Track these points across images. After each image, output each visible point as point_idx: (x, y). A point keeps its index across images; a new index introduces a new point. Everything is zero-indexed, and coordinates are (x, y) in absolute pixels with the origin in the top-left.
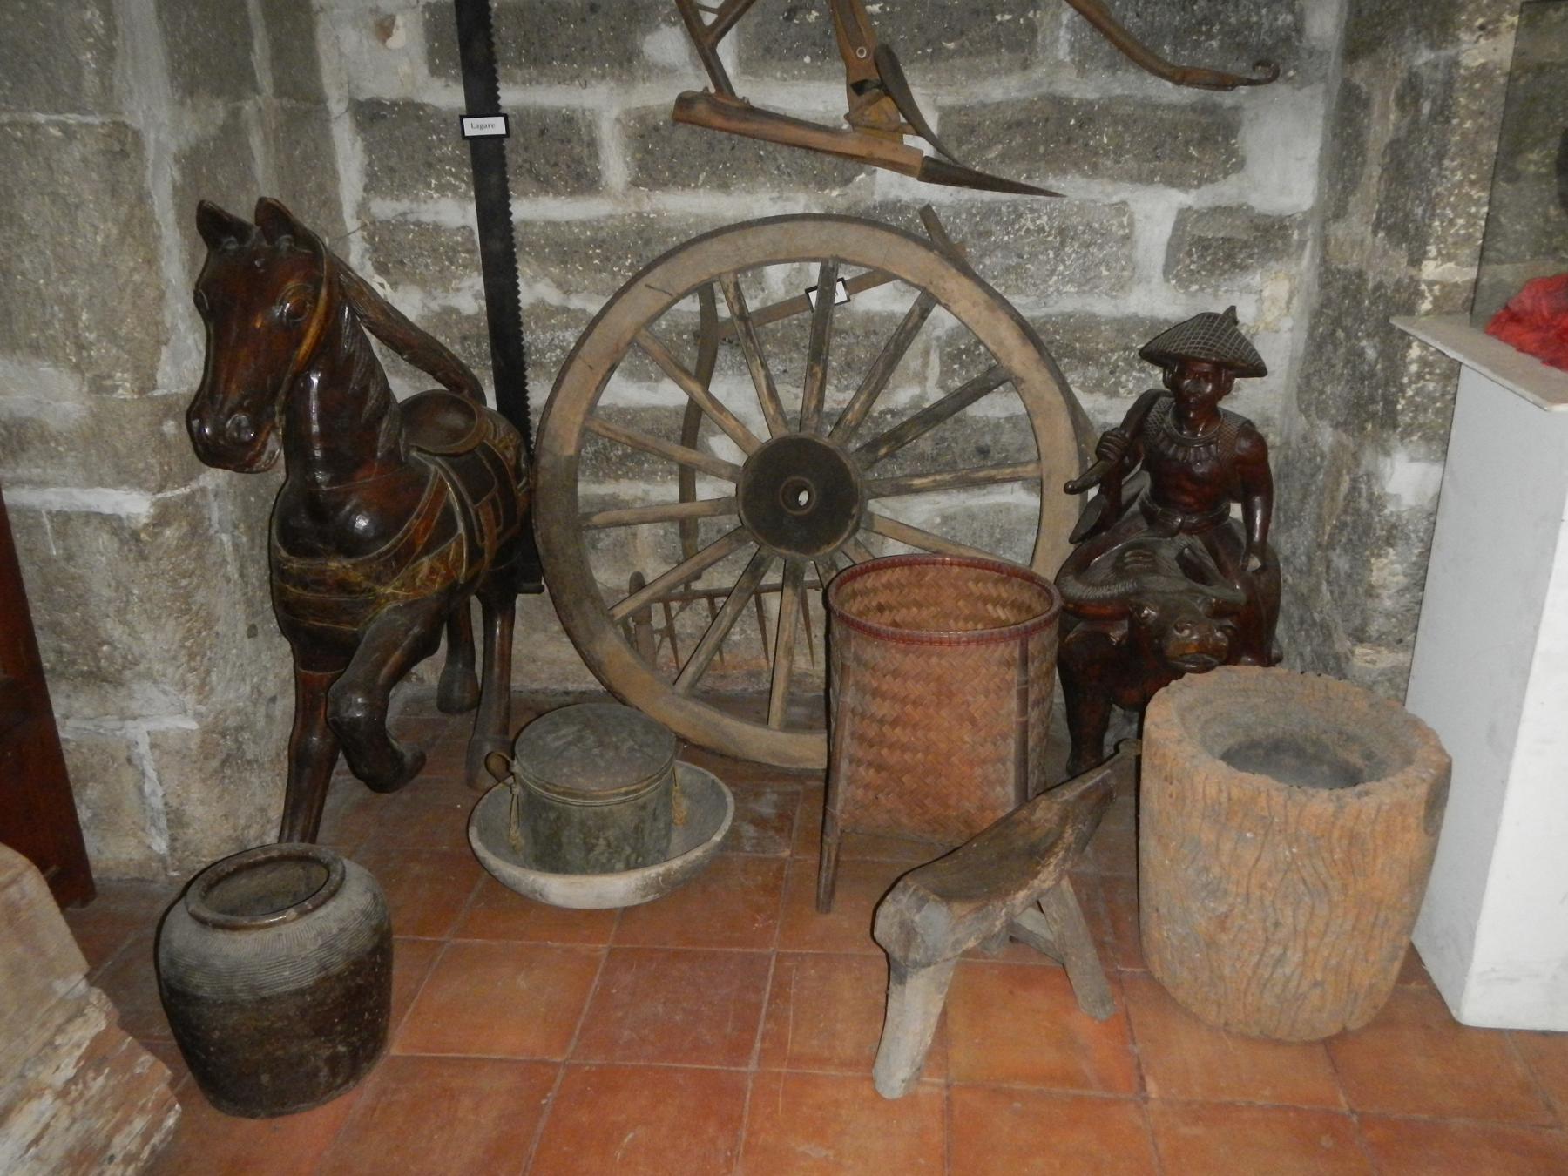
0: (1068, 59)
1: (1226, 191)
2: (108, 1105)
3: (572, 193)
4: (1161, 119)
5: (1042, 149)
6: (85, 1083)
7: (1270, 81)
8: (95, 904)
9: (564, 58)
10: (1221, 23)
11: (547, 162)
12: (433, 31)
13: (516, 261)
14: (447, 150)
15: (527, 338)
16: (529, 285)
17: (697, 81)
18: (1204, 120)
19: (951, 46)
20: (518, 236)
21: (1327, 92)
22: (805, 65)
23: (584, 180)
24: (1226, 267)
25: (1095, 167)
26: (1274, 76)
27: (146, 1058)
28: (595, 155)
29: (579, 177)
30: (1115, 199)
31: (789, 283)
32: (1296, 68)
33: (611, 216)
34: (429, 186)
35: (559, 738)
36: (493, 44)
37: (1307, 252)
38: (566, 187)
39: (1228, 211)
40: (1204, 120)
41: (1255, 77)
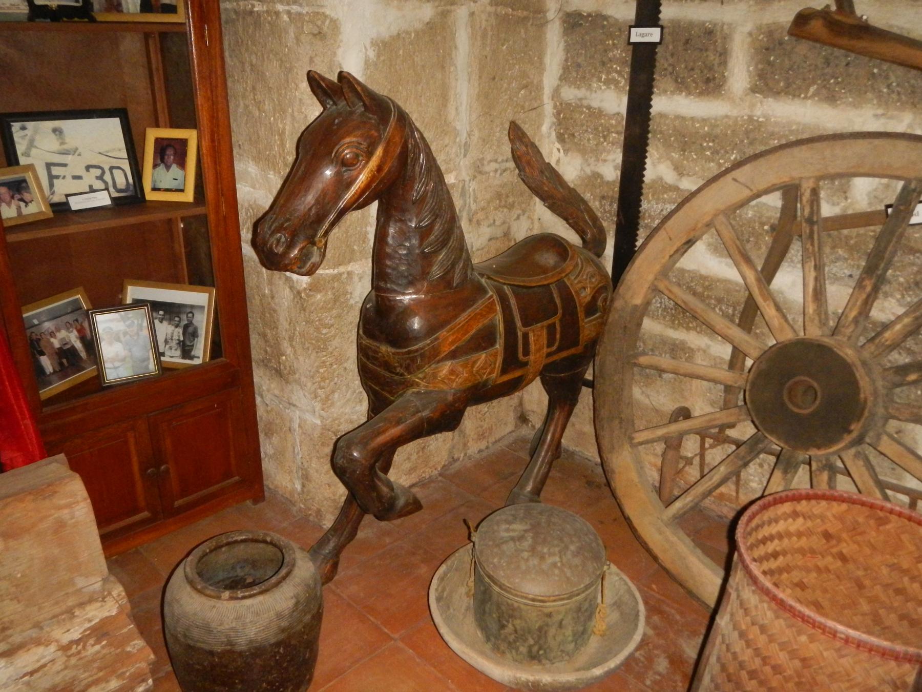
2: (96, 665)
3: (701, 94)
6: (84, 647)
8: (261, 505)
11: (686, 67)
13: (647, 145)
14: (617, 53)
15: (645, 205)
16: (654, 165)
20: (652, 125)
23: (711, 83)
27: (139, 643)
28: (724, 63)
29: (708, 81)
31: (874, 196)
33: (727, 116)
34: (600, 80)
35: (508, 530)
38: (696, 88)
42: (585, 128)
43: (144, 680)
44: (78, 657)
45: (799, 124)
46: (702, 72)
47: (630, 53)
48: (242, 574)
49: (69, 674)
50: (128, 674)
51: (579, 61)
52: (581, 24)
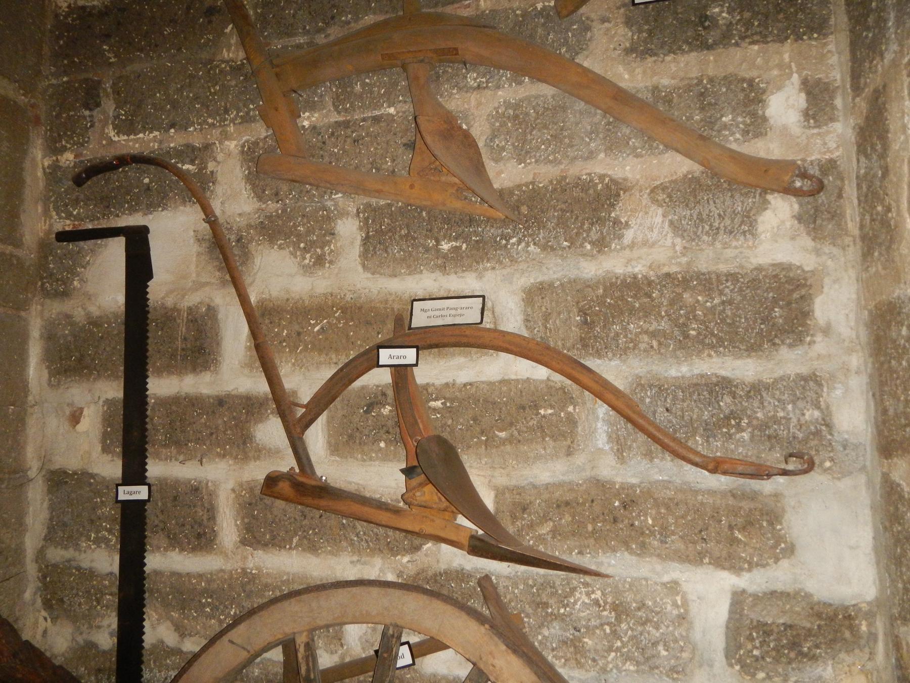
0: (607, 447)
1: (777, 576)
3: (194, 550)
4: (702, 504)
5: (590, 528)
7: (805, 472)
9: (198, 441)
10: (749, 417)
12: (107, 420)
13: (144, 606)
14: (106, 510)
16: (153, 627)
17: (287, 463)
18: (746, 505)
19: (503, 435)
21: (870, 483)
22: (381, 449)
23: (202, 538)
24: (792, 655)
25: (643, 546)
26: (810, 466)
28: (212, 518)
29: (199, 536)
30: (666, 579)
31: (366, 643)
32: (832, 460)
33: (222, 571)
36: (146, 430)
37: (880, 647)
39: (784, 596)
40: (746, 505)
41: (790, 467)
42: (74, 591)
45: (288, 574)
46: (192, 527)
47: (119, 511)
51: (65, 519)
52: (67, 482)
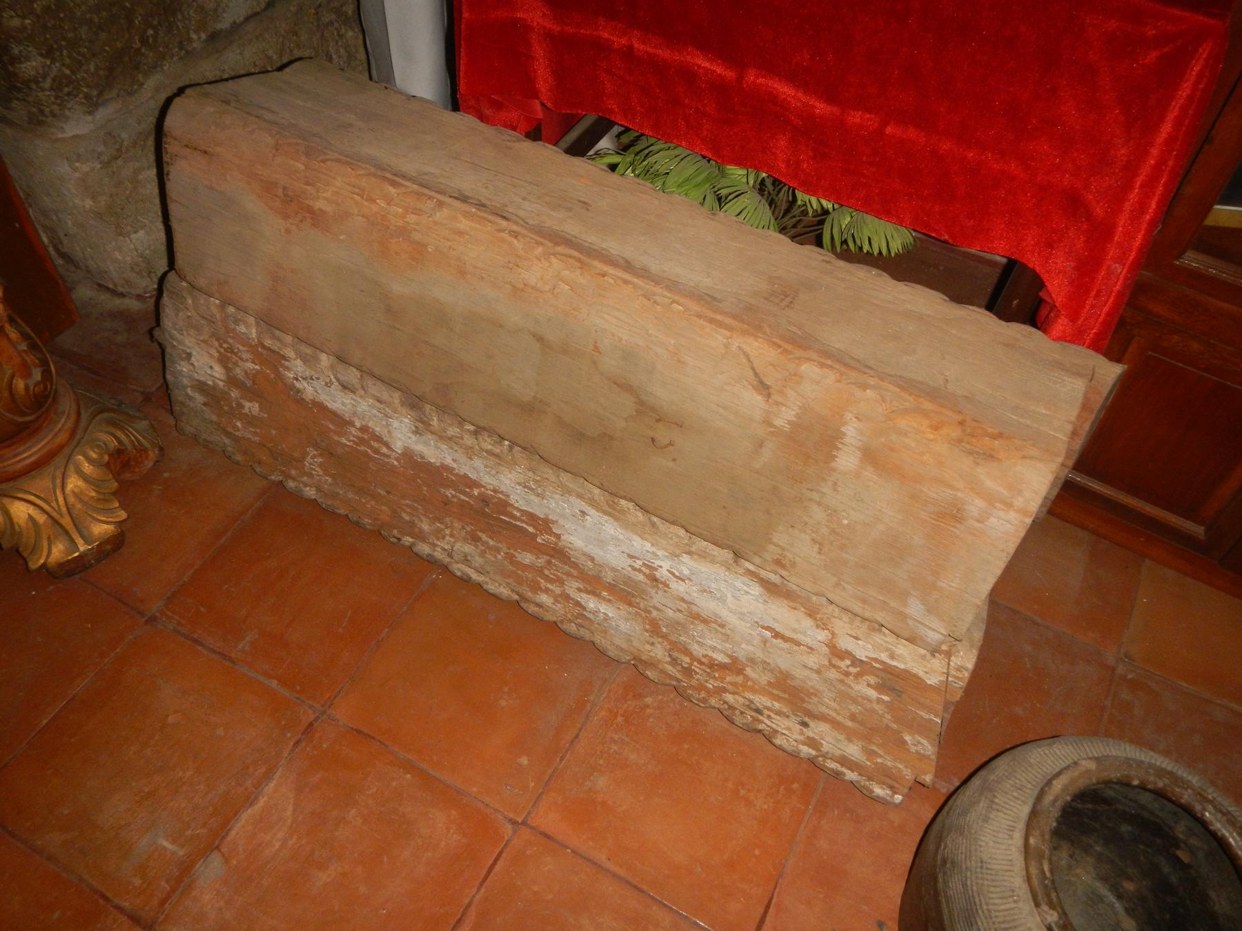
2: (853, 708)
6: (857, 676)
27: (927, 747)
43: (891, 787)
44: (842, 677)
48: (1181, 836)
49: (814, 681)
50: (879, 760)
